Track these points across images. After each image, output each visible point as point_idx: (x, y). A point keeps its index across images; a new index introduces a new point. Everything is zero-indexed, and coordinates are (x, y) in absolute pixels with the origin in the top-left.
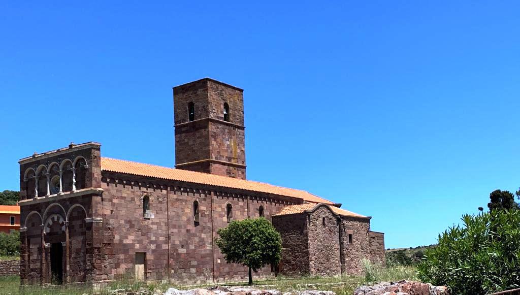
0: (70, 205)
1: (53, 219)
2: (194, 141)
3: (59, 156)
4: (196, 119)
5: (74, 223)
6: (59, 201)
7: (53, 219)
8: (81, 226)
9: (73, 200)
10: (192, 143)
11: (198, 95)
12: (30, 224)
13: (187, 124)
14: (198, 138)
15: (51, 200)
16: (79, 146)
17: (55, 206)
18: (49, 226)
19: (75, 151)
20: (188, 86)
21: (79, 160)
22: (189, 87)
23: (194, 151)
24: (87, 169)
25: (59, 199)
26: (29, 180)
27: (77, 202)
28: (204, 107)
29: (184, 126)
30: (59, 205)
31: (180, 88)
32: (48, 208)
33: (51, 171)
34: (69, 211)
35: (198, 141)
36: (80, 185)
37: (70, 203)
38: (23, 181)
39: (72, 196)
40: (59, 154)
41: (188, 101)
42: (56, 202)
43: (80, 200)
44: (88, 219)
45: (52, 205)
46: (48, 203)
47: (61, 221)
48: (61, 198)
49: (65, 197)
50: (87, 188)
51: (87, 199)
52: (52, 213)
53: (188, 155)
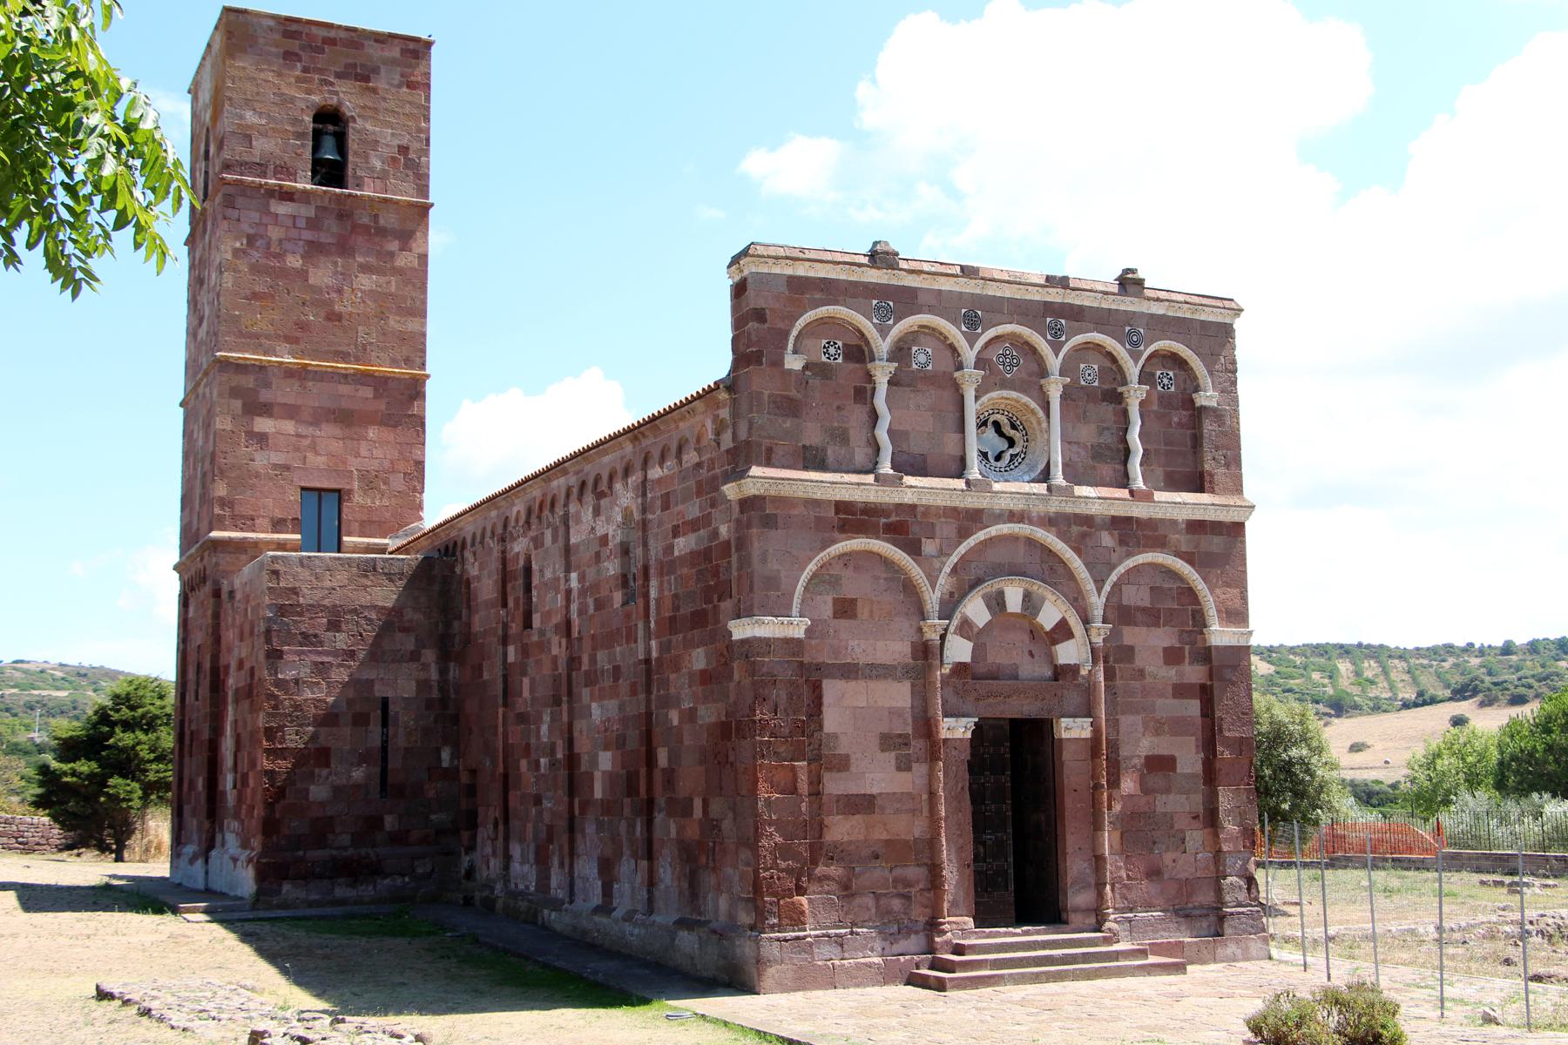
0: (1121, 550)
1: (996, 603)
2: (346, 276)
3: (1049, 308)
4: (359, 186)
5: (1132, 635)
6: (1050, 522)
7: (996, 603)
8: (1172, 656)
9: (1130, 531)
10: (329, 281)
11: (374, 91)
12: (826, 609)
13: (305, 191)
14: (366, 269)
15: (1004, 504)
16: (1180, 298)
17: (1013, 539)
18: (966, 628)
19: (1152, 316)
20: (323, 33)
22: (332, 42)
23: (334, 317)
24: (1214, 410)
25: (1055, 506)
26: (806, 367)
28: (404, 150)
29: (287, 196)
31: (271, 23)
32: (971, 542)
33: (980, 363)
34: (1113, 577)
35: (366, 282)
39: (1139, 511)
40: (1055, 296)
41: (316, 98)
42: (1031, 523)
43: (1183, 541)
44: (1220, 634)
45: (994, 531)
46: (970, 520)
47: (1049, 617)
48: (1069, 509)
49: (1095, 509)
50: (1212, 491)
51: (1216, 543)
53: (303, 326)
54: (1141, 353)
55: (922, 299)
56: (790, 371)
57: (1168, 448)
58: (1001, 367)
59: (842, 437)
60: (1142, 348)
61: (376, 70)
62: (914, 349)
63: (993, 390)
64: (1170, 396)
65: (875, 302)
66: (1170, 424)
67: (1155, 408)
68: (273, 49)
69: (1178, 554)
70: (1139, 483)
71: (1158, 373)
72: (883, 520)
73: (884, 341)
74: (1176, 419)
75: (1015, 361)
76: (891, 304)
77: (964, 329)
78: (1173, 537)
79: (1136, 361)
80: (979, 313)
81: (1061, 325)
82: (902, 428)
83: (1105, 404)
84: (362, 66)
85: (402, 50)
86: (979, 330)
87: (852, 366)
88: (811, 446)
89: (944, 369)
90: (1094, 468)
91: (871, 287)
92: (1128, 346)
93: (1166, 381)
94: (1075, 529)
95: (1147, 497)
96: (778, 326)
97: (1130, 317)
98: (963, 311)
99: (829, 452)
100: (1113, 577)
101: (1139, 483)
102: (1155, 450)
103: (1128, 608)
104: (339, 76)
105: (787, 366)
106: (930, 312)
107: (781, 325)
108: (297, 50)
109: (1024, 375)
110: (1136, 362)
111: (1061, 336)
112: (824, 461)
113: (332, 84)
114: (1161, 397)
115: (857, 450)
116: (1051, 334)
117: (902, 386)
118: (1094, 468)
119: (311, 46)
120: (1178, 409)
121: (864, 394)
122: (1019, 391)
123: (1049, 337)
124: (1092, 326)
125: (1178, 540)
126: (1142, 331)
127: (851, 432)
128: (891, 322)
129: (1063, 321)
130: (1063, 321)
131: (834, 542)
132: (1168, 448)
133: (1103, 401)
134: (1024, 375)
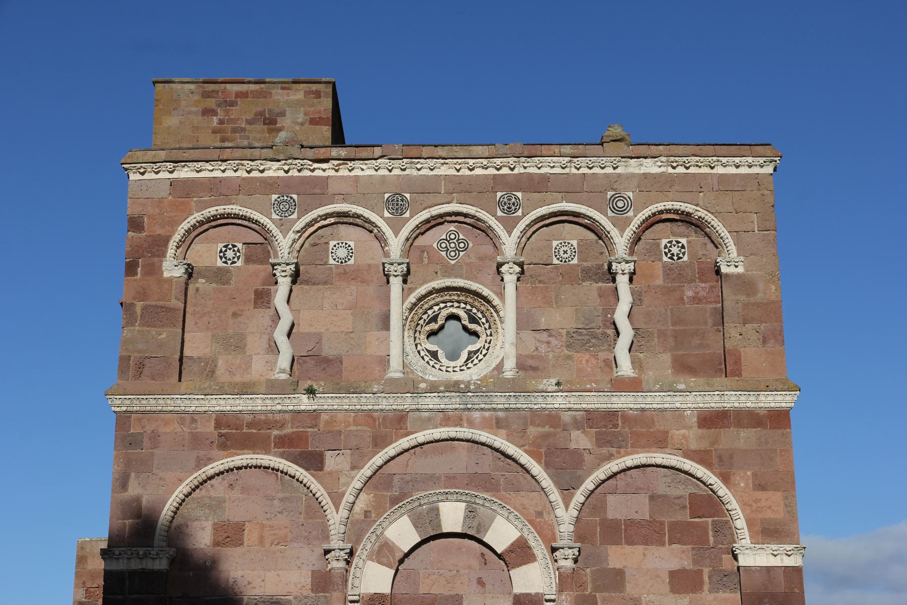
19: (646, 176)
21: (649, 223)
27: (661, 442)
30: (500, 442)
36: (667, 358)
37: (601, 441)
38: (154, 270)
39: (623, 402)
42: (471, 424)
52: (431, 480)
54: (629, 221)
55: (333, 188)
56: (170, 280)
57: (678, 328)
58: (444, 254)
59: (237, 344)
60: (631, 214)
61: (283, 114)
62: (332, 243)
63: (433, 280)
64: (682, 267)
65: (274, 197)
66: (682, 299)
67: (659, 282)
68: (193, 109)
69: (688, 454)
70: (626, 368)
71: (664, 242)
72: (276, 432)
73: (284, 238)
74: (690, 293)
75: (462, 245)
76: (295, 197)
77: (387, 214)
78: (677, 434)
79: (622, 231)
80: (408, 196)
81: (517, 198)
82: (312, 330)
83: (588, 283)
84: (270, 111)
85: (307, 93)
86: (407, 215)
87: (253, 267)
88: (199, 358)
89: (370, 262)
90: (569, 357)
91: (271, 182)
92: (610, 213)
93: (675, 250)
94: (533, 431)
95: (633, 386)
96: (158, 233)
97: (613, 182)
98: (387, 196)
99: (220, 363)
100: (589, 484)
101: (626, 368)
102: (659, 331)
103: (616, 523)
104: (249, 122)
105: (166, 275)
106: (344, 200)
107: (159, 231)
108: (213, 106)
109: (473, 259)
110: (622, 231)
111: (516, 210)
112: (213, 372)
113: (243, 130)
114: (668, 271)
115: (255, 358)
116: (503, 211)
117: (314, 284)
118: (569, 357)
119: (226, 101)
120: (692, 281)
121: (263, 298)
122: (467, 278)
123: (500, 213)
124: (559, 195)
125: (684, 436)
126: (631, 194)
127: (250, 339)
128: (295, 216)
129: (519, 195)
130: (519, 195)
131: (210, 460)
132: (678, 328)
133: (583, 281)
134: (473, 259)
